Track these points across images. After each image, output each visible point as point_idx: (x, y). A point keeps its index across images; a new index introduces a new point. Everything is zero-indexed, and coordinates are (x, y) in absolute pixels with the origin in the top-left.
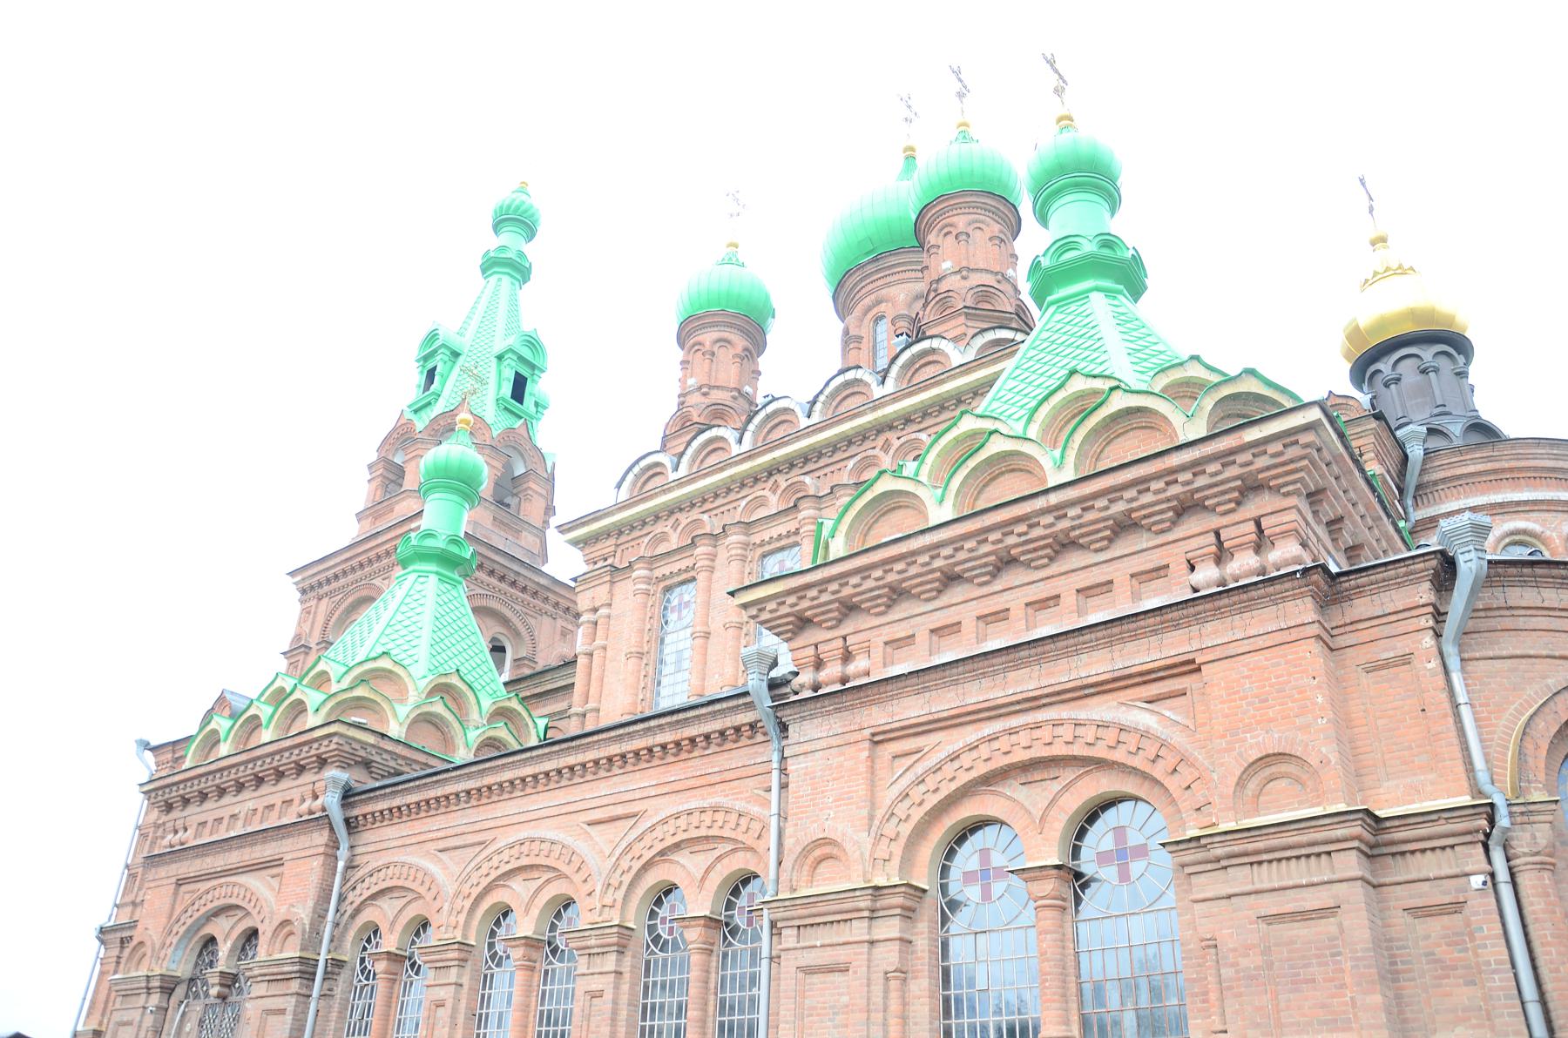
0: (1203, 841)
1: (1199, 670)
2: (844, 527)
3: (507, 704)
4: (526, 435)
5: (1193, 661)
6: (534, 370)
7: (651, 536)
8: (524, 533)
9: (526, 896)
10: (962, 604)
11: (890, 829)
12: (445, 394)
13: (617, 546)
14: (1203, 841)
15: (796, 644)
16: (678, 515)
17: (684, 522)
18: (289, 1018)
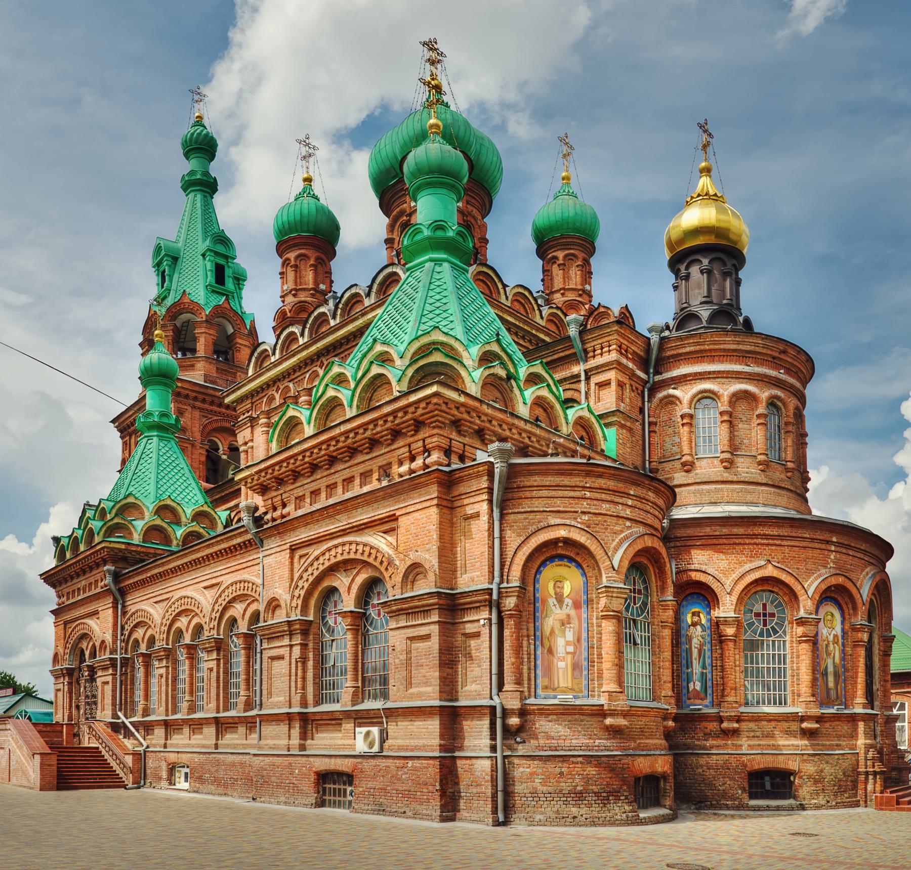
0: (389, 603)
1: (397, 519)
2: (276, 436)
3: (202, 509)
4: (228, 307)
5: (394, 515)
6: (227, 259)
7: (310, 372)
8: (239, 374)
9: (186, 624)
10: (320, 480)
11: (296, 593)
12: (174, 287)
13: (252, 403)
14: (389, 603)
15: (266, 498)
16: (278, 383)
17: (282, 387)
18: (110, 684)
